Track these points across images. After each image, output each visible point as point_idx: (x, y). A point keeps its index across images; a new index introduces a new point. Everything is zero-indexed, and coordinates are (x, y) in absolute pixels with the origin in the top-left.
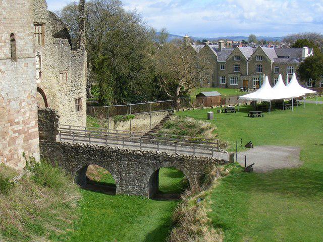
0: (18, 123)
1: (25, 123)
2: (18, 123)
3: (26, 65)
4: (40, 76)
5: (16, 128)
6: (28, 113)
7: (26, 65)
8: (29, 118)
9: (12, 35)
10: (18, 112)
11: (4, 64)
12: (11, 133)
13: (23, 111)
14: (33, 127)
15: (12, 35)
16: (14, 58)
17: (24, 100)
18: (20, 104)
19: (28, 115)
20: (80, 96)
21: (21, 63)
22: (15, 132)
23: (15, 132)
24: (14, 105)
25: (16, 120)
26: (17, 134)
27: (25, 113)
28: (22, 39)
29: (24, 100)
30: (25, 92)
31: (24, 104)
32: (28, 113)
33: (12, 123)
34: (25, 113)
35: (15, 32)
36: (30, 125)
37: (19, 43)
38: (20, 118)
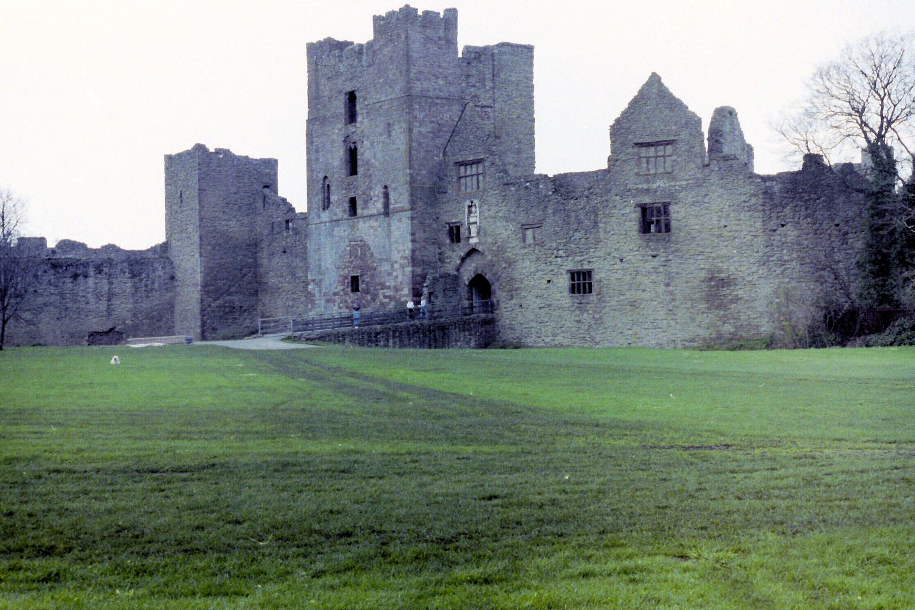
0: (389, 288)
1: (397, 289)
2: (389, 288)
3: (400, 220)
4: (478, 233)
5: (388, 292)
6: (400, 277)
7: (400, 220)
8: (401, 283)
9: (386, 187)
10: (389, 274)
11: (377, 220)
12: (381, 297)
13: (395, 274)
14: (405, 295)
15: (386, 187)
16: (387, 213)
17: (396, 262)
18: (392, 266)
19: (400, 280)
20: (586, 267)
21: (396, 217)
22: (386, 297)
23: (386, 297)
24: (386, 267)
25: (388, 284)
26: (387, 300)
27: (397, 277)
28: (395, 189)
29: (396, 262)
30: (399, 252)
31: (396, 266)
32: (400, 277)
33: (383, 286)
34: (397, 277)
35: (388, 183)
36: (403, 293)
37: (393, 197)
38: (390, 283)
